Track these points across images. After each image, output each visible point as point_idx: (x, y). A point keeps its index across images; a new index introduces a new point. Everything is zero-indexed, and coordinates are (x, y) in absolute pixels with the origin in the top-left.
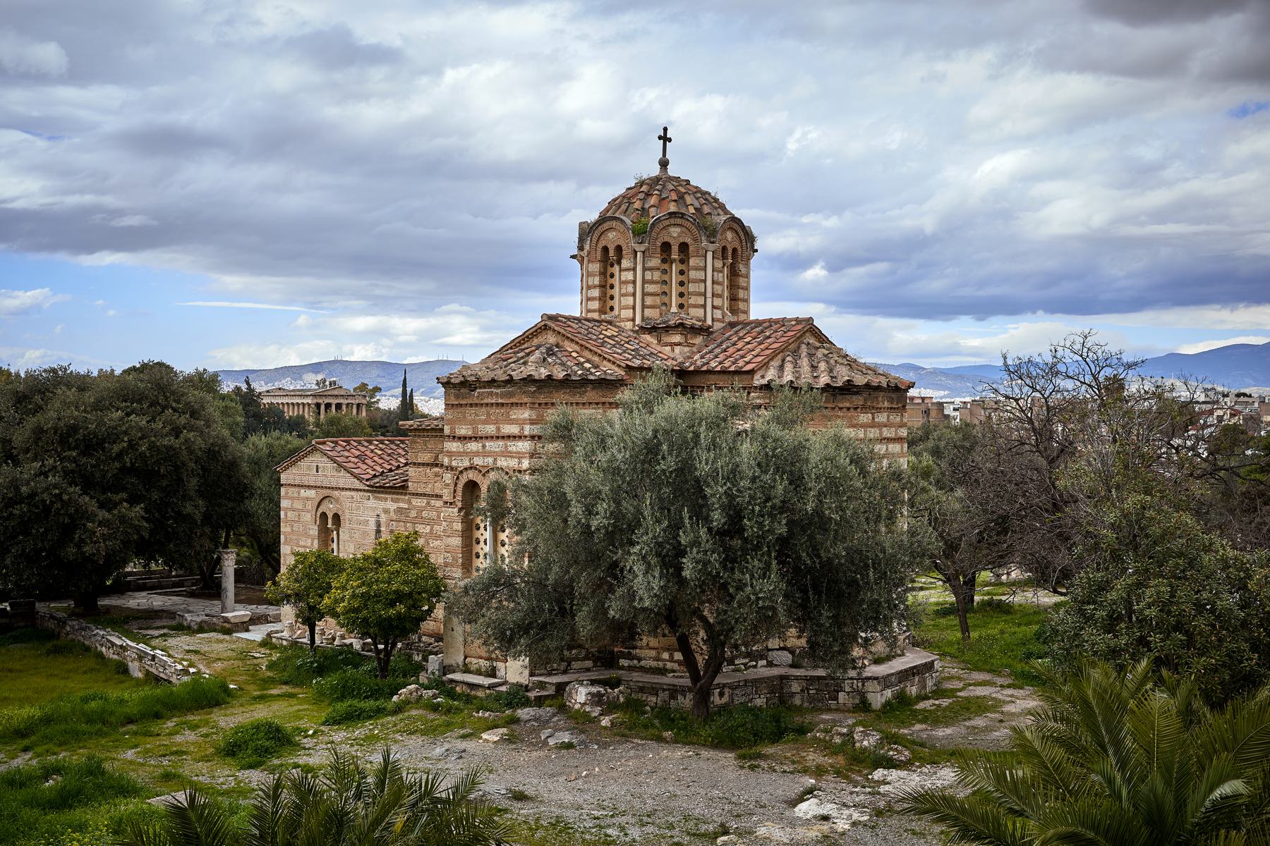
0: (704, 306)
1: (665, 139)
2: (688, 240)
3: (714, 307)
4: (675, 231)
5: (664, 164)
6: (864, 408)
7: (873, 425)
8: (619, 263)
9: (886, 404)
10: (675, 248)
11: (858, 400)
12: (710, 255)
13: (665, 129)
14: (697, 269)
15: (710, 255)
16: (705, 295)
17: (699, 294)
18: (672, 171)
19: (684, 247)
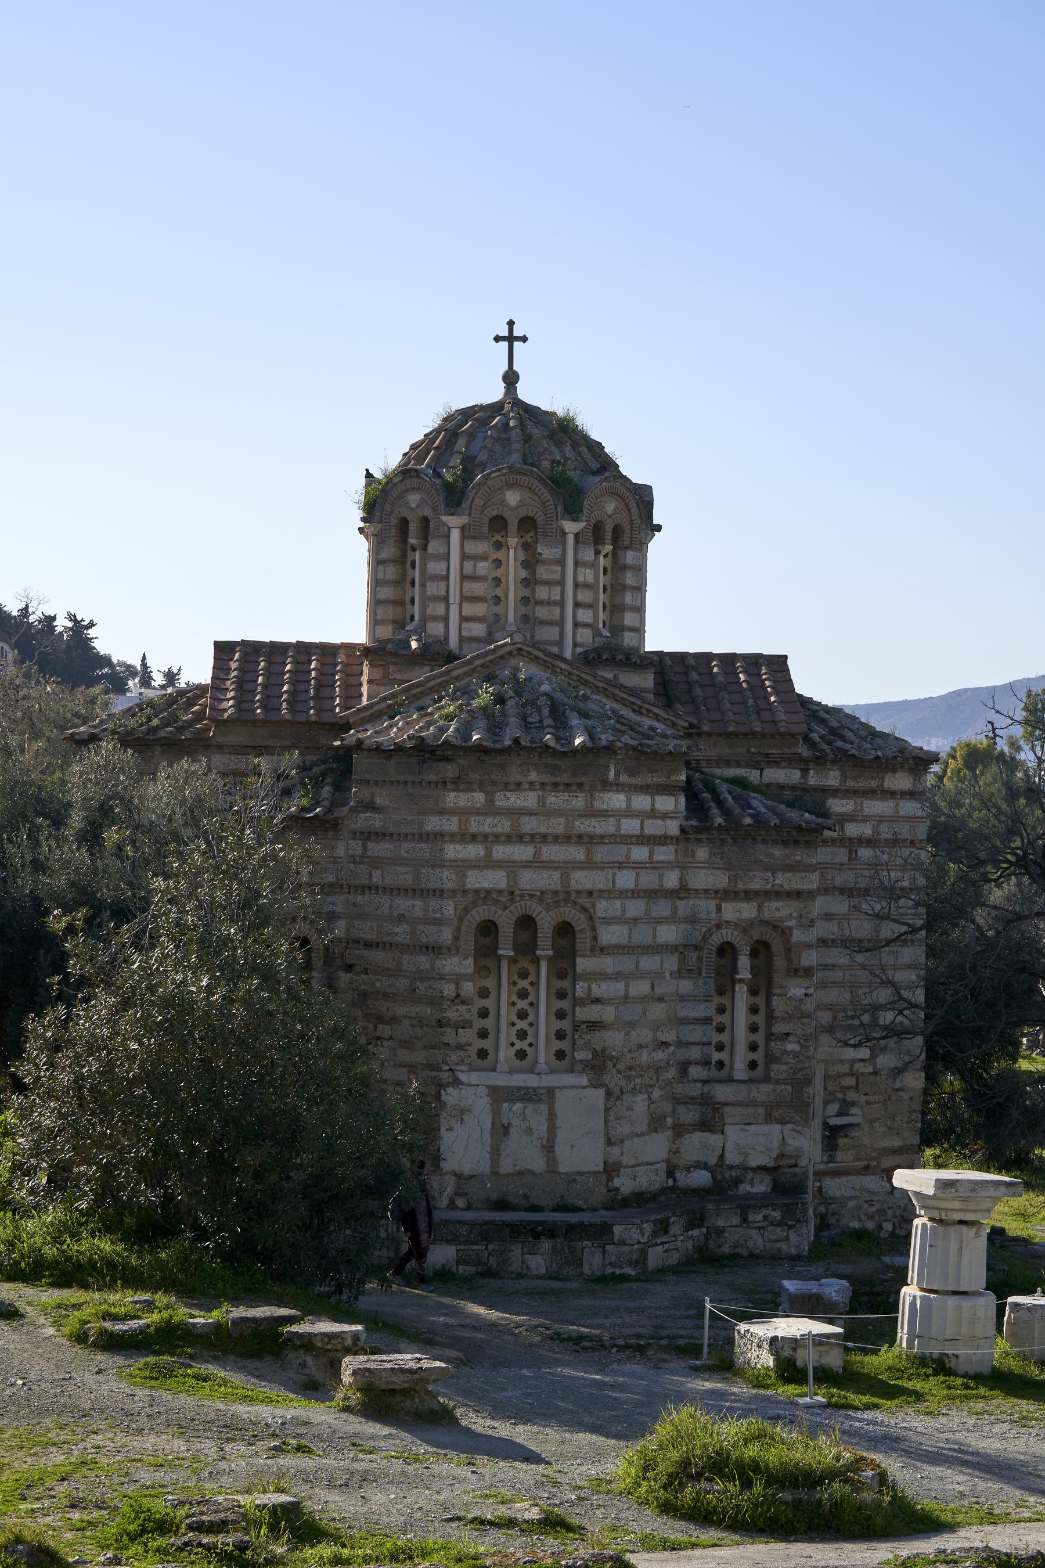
0: (446, 619)
1: (511, 339)
2: (428, 512)
3: (464, 619)
4: (414, 499)
5: (511, 378)
6: (458, 783)
7: (490, 810)
8: (425, 548)
9: (533, 776)
10: (413, 527)
11: (450, 771)
12: (455, 535)
13: (511, 324)
14: (437, 557)
15: (455, 535)
16: (446, 599)
17: (436, 598)
18: (526, 393)
19: (425, 521)
